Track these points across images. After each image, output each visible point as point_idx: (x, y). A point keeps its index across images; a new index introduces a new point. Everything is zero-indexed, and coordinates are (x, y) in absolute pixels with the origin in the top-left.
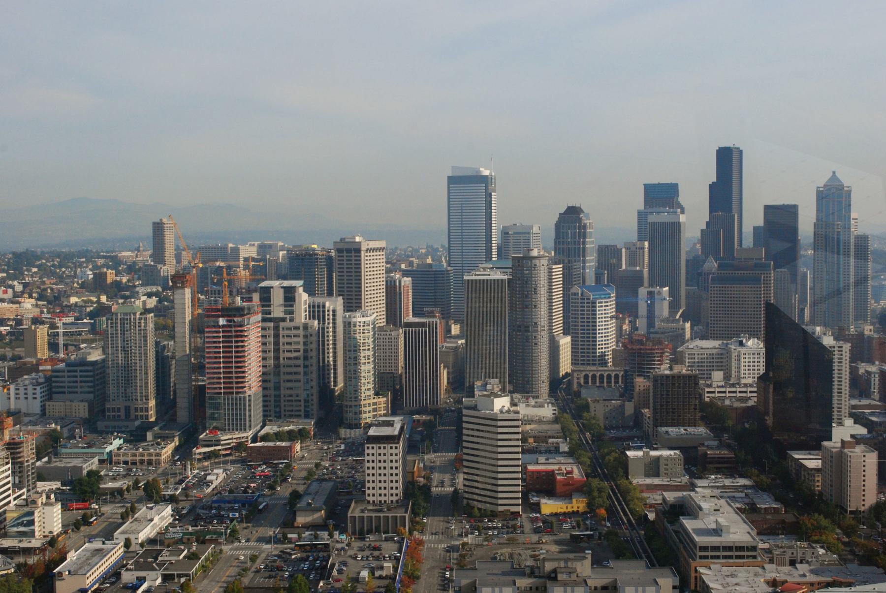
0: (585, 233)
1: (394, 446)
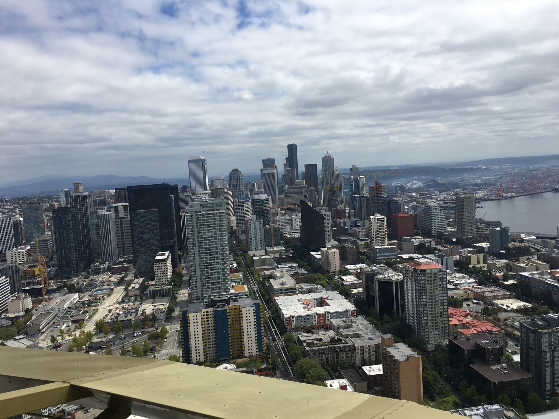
0: (239, 179)
1: (165, 263)
